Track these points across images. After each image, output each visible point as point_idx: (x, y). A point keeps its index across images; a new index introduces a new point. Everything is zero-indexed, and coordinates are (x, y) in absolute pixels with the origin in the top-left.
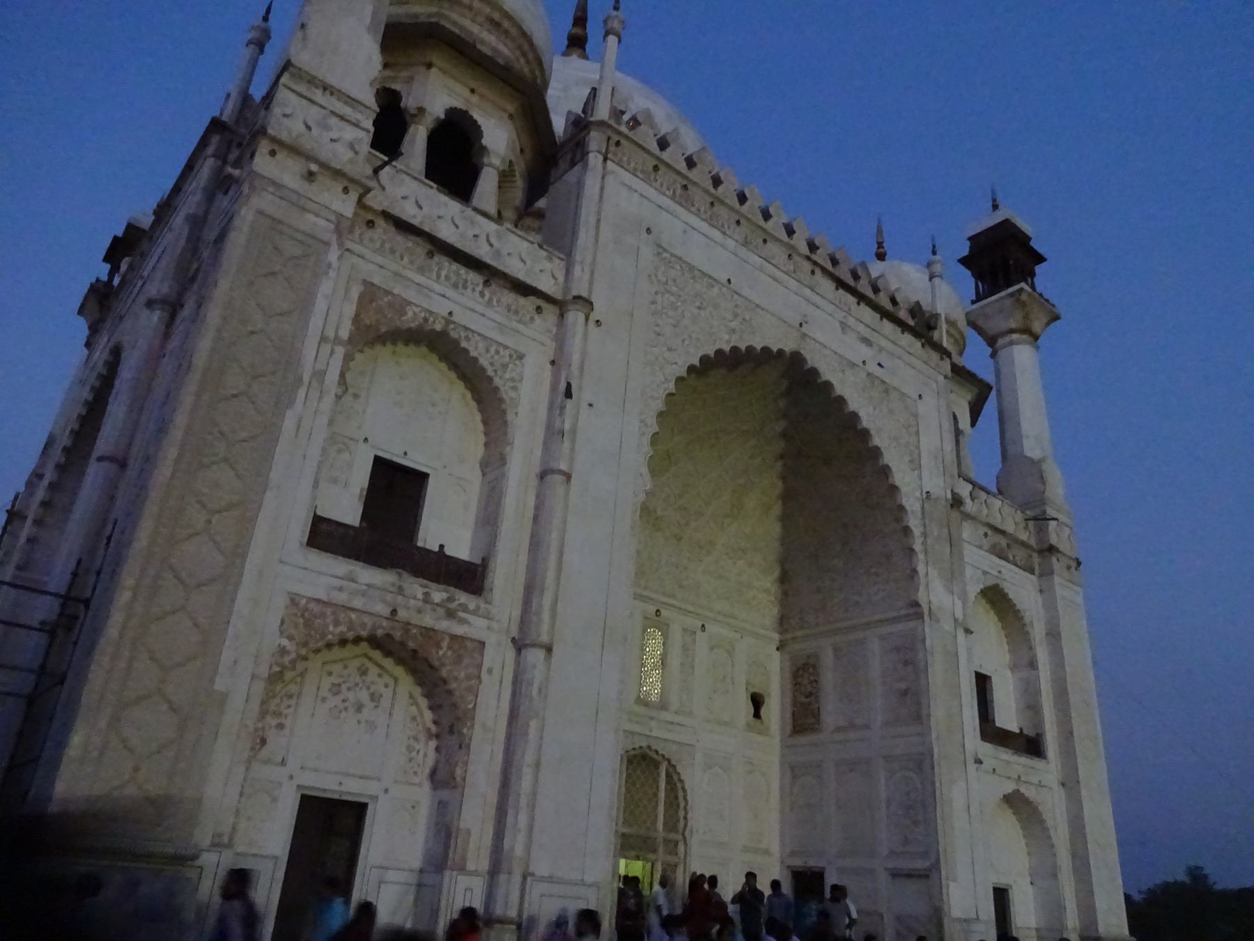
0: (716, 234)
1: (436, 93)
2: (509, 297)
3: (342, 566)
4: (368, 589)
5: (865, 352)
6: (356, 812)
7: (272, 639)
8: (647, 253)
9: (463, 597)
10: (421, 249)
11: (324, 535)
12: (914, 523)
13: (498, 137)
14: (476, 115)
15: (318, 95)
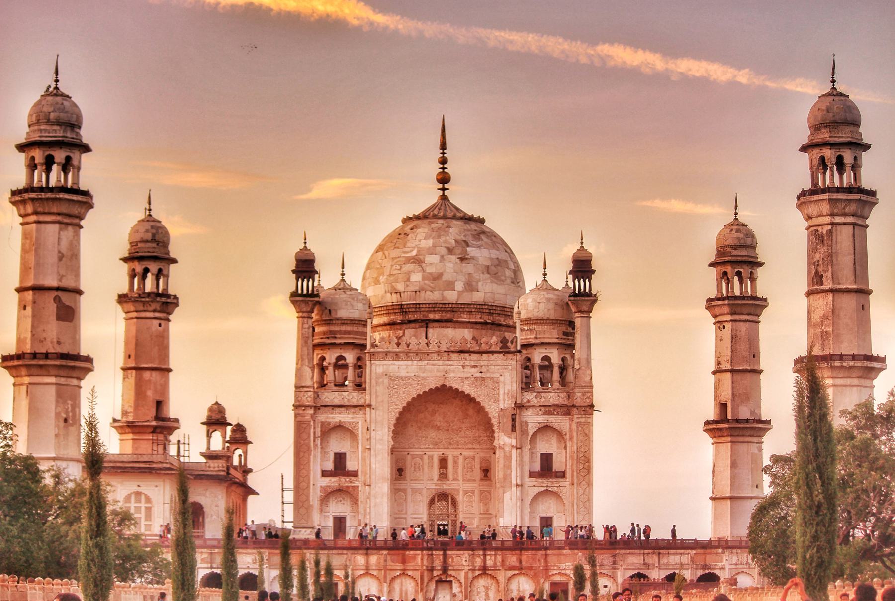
0: (410, 362)
1: (331, 356)
2: (353, 410)
3: (328, 479)
4: (333, 482)
5: (473, 370)
6: (344, 518)
7: (319, 493)
8: (386, 381)
9: (353, 478)
10: (330, 409)
11: (325, 474)
12: (494, 422)
13: (350, 357)
14: (343, 354)
15: (302, 390)
